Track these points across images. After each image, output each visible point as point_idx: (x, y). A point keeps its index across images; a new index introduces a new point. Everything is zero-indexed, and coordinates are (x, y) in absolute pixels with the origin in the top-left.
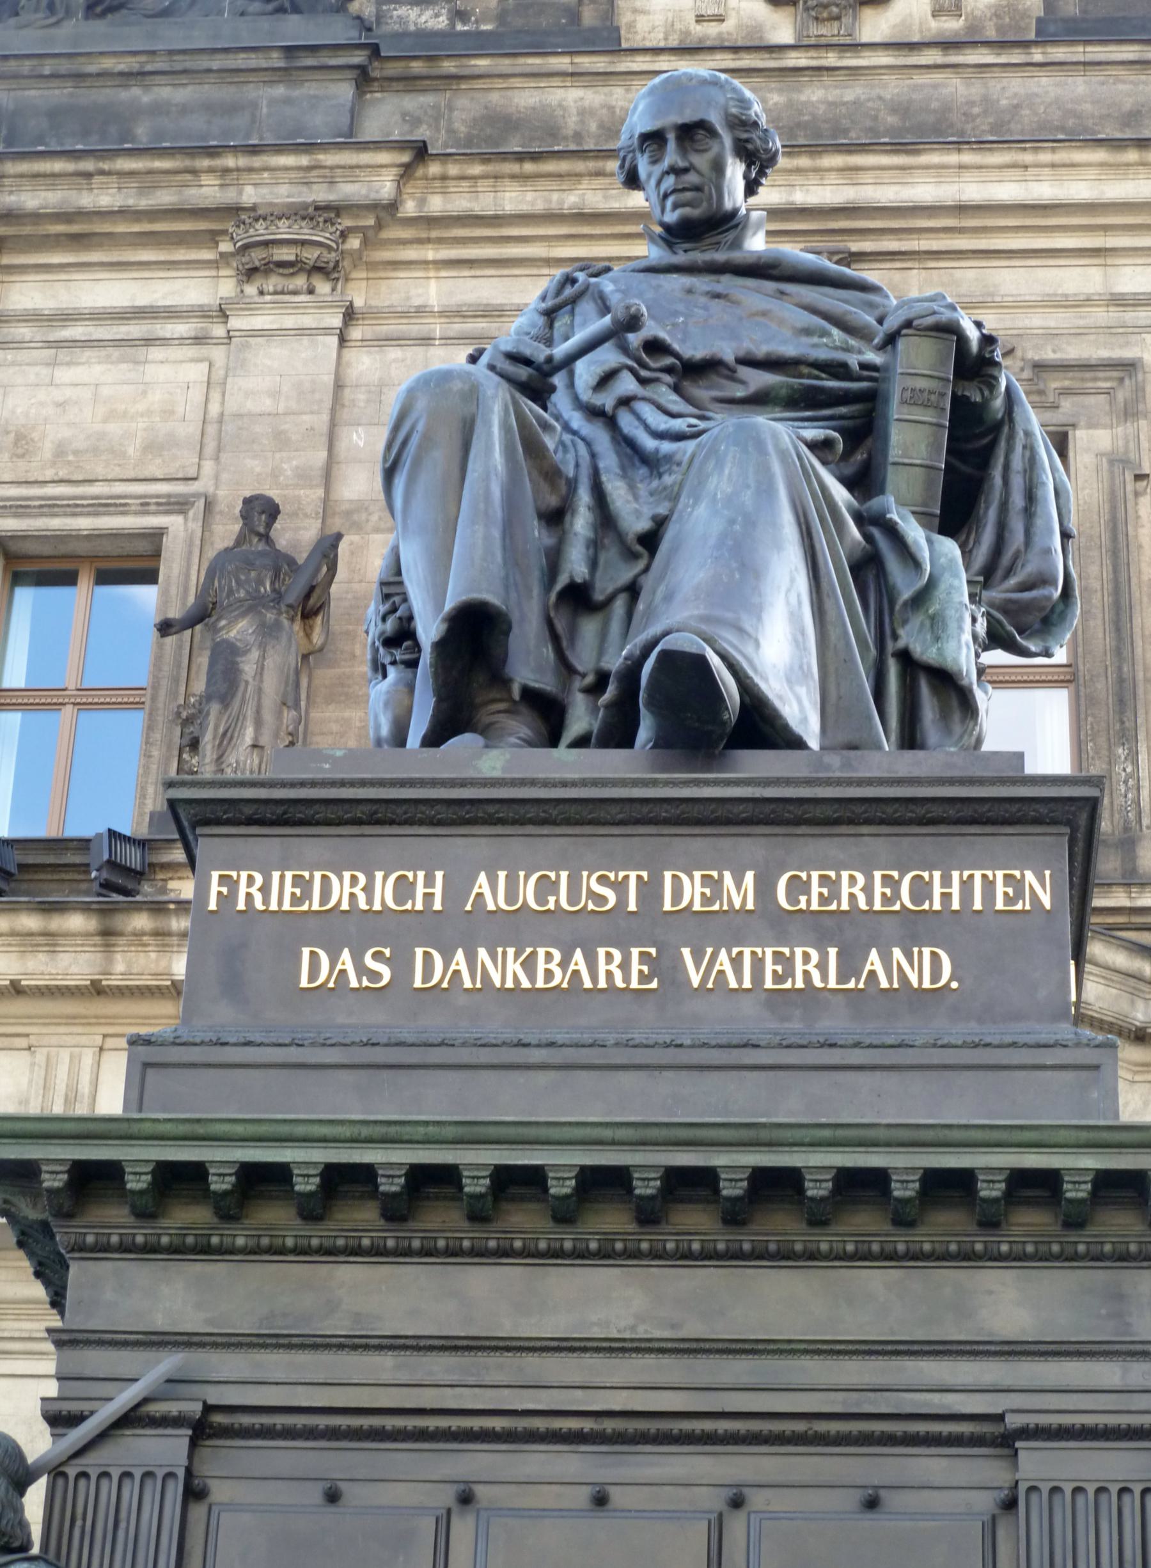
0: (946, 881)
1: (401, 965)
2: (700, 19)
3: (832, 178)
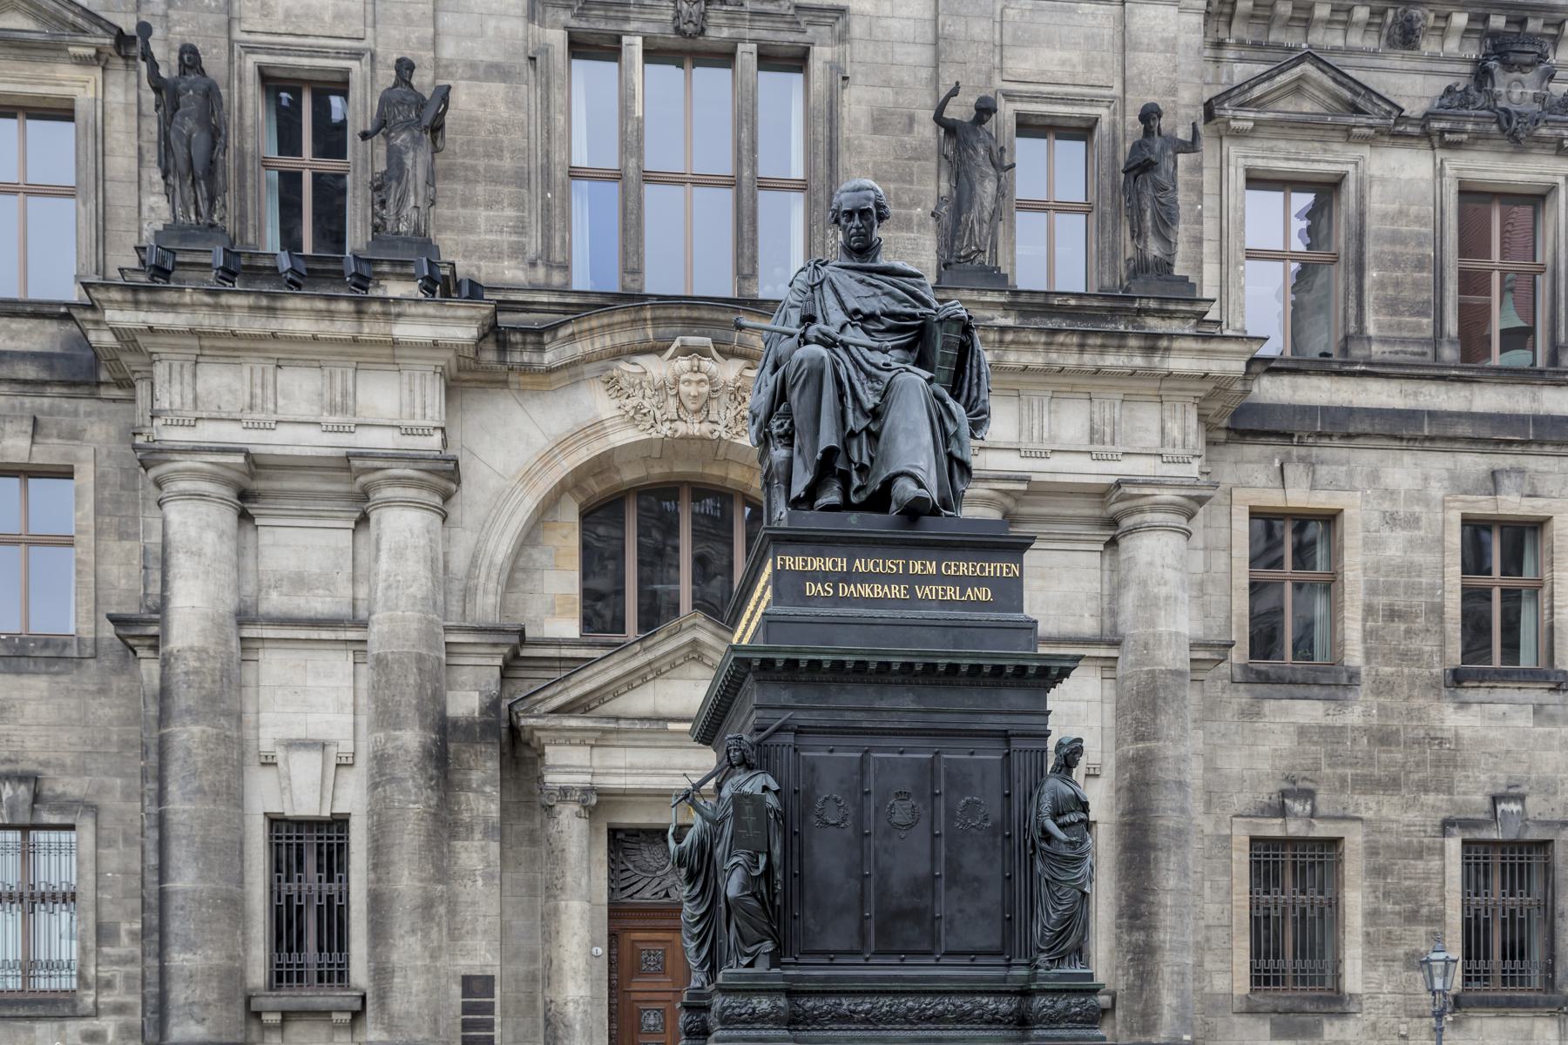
1: (836, 588)
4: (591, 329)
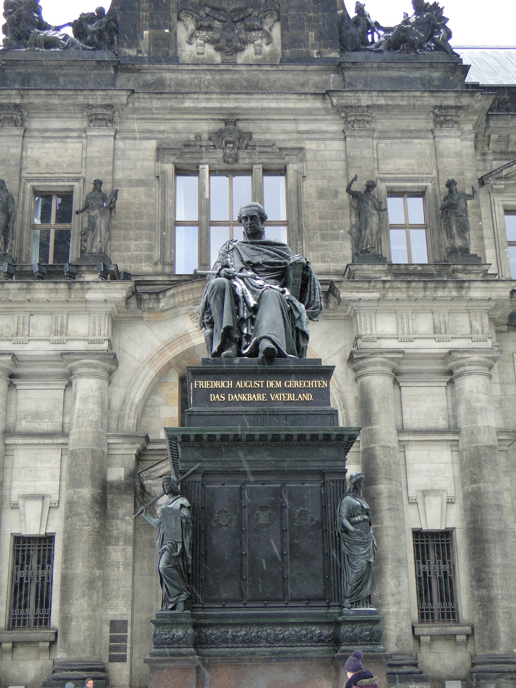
1: (226, 397)
2: (198, 54)
3: (232, 101)
4: (183, 292)
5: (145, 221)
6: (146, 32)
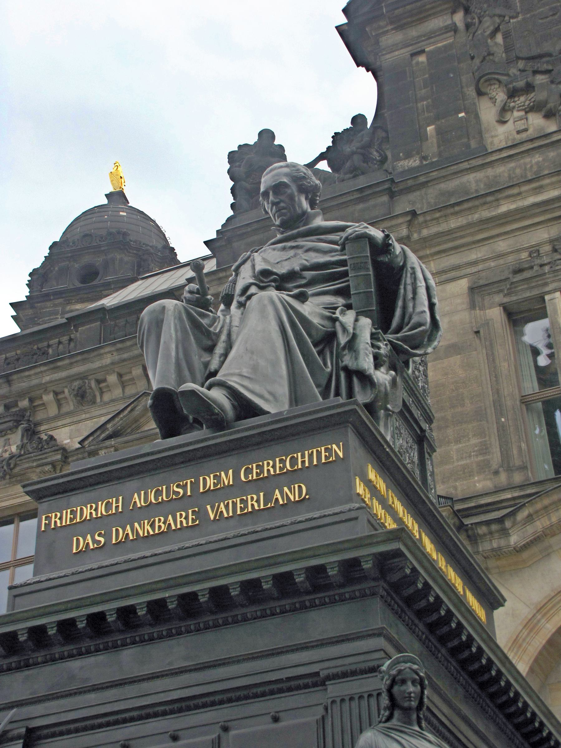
0: (303, 456)
1: (108, 536)
2: (518, 132)
5: (469, 407)
6: (430, 129)
